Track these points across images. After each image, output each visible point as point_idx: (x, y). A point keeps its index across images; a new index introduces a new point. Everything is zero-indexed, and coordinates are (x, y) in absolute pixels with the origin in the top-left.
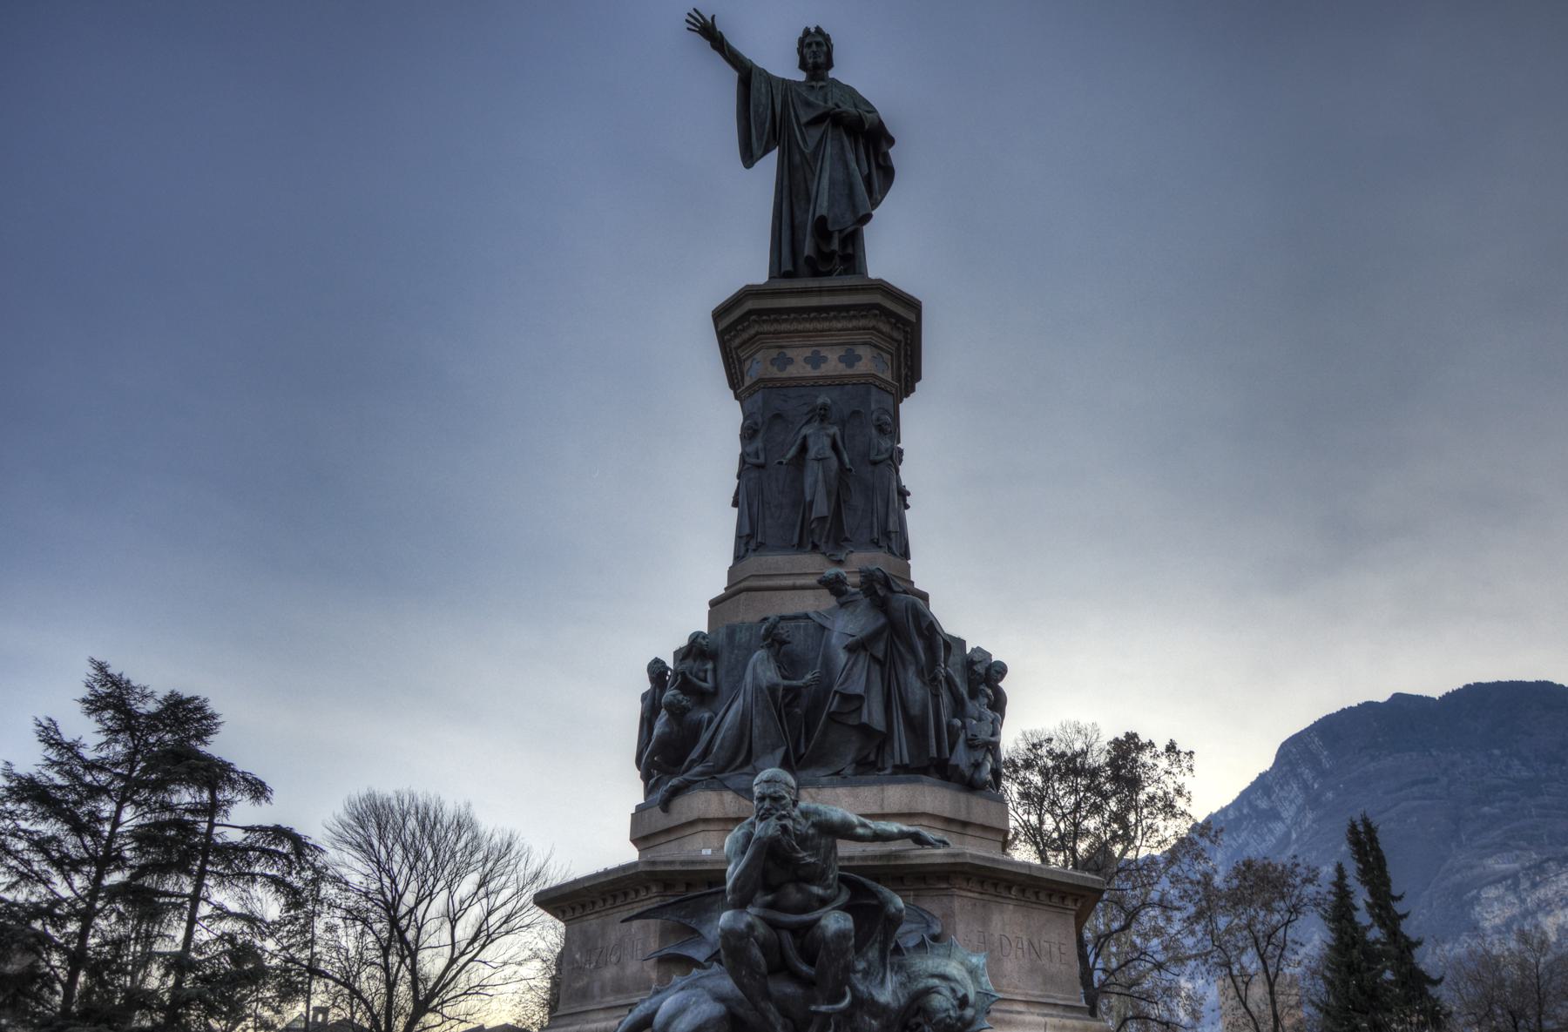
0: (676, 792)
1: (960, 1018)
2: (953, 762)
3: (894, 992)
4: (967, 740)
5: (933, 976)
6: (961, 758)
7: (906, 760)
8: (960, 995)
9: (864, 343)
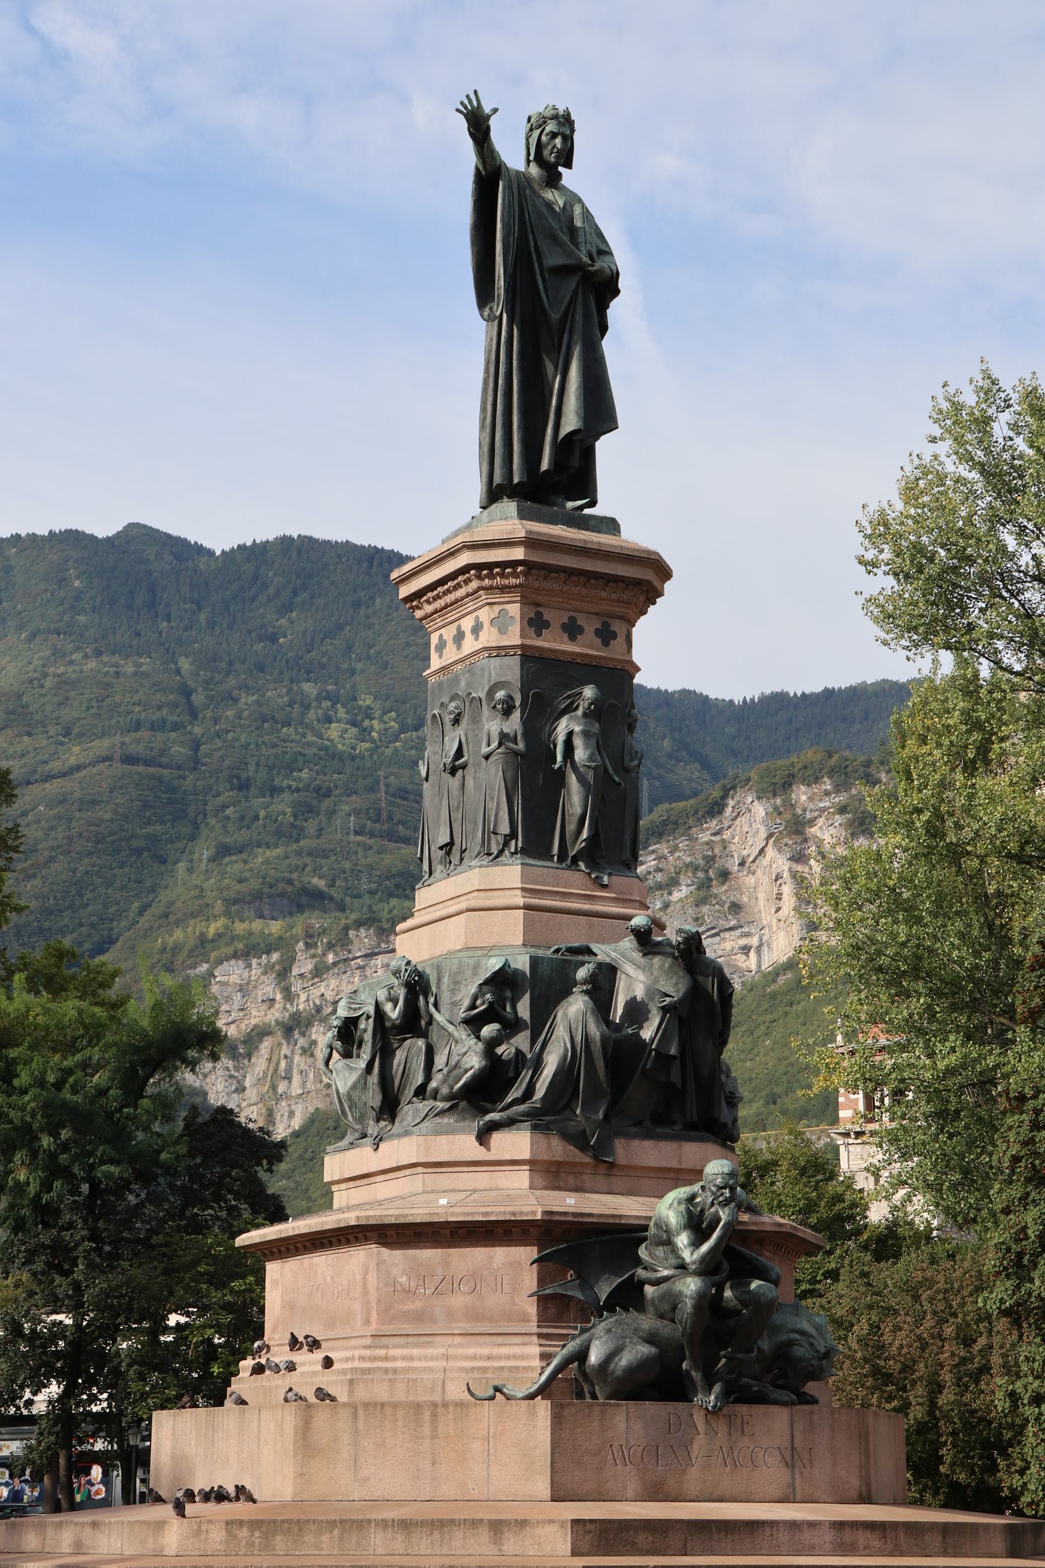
0: (494, 1127)
4: (726, 1097)
9: (620, 618)
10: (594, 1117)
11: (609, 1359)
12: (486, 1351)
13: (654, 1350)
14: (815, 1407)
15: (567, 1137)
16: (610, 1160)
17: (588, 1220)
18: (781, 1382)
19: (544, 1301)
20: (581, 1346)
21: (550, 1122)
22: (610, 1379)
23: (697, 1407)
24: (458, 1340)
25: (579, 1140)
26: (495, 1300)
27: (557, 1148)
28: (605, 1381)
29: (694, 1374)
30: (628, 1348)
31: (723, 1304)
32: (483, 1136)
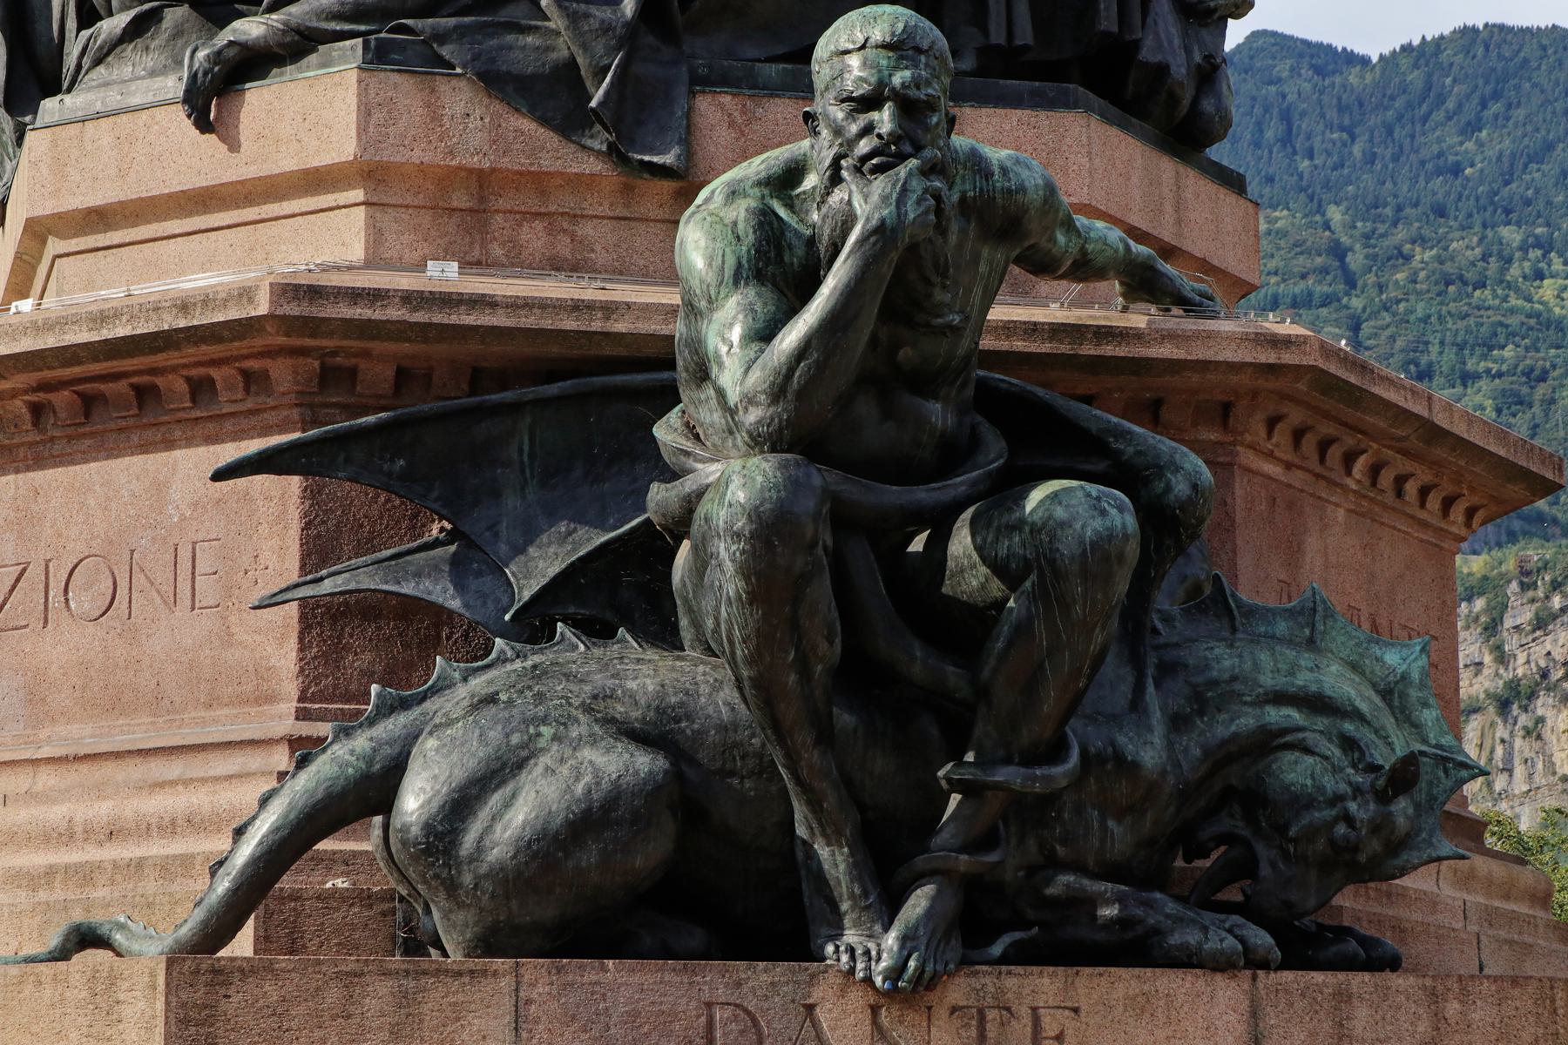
0: (250, 65)
1: (1380, 826)
2: (1147, 54)
3: (1170, 746)
5: (1280, 698)
6: (1164, 40)
7: (1025, 34)
8: (1384, 757)
10: (602, 13)
11: (460, 805)
12: (103, 810)
13: (645, 763)
14: (1397, 981)
15: (496, 81)
16: (668, 159)
17: (469, 319)
18: (1233, 894)
19: (327, 625)
20: (370, 761)
21: (441, 37)
22: (467, 879)
23: (834, 979)
24: (47, 779)
25: (553, 97)
26: (170, 636)
27: (465, 123)
28: (452, 888)
29: (823, 851)
30: (545, 760)
31: (946, 589)
32: (211, 99)
